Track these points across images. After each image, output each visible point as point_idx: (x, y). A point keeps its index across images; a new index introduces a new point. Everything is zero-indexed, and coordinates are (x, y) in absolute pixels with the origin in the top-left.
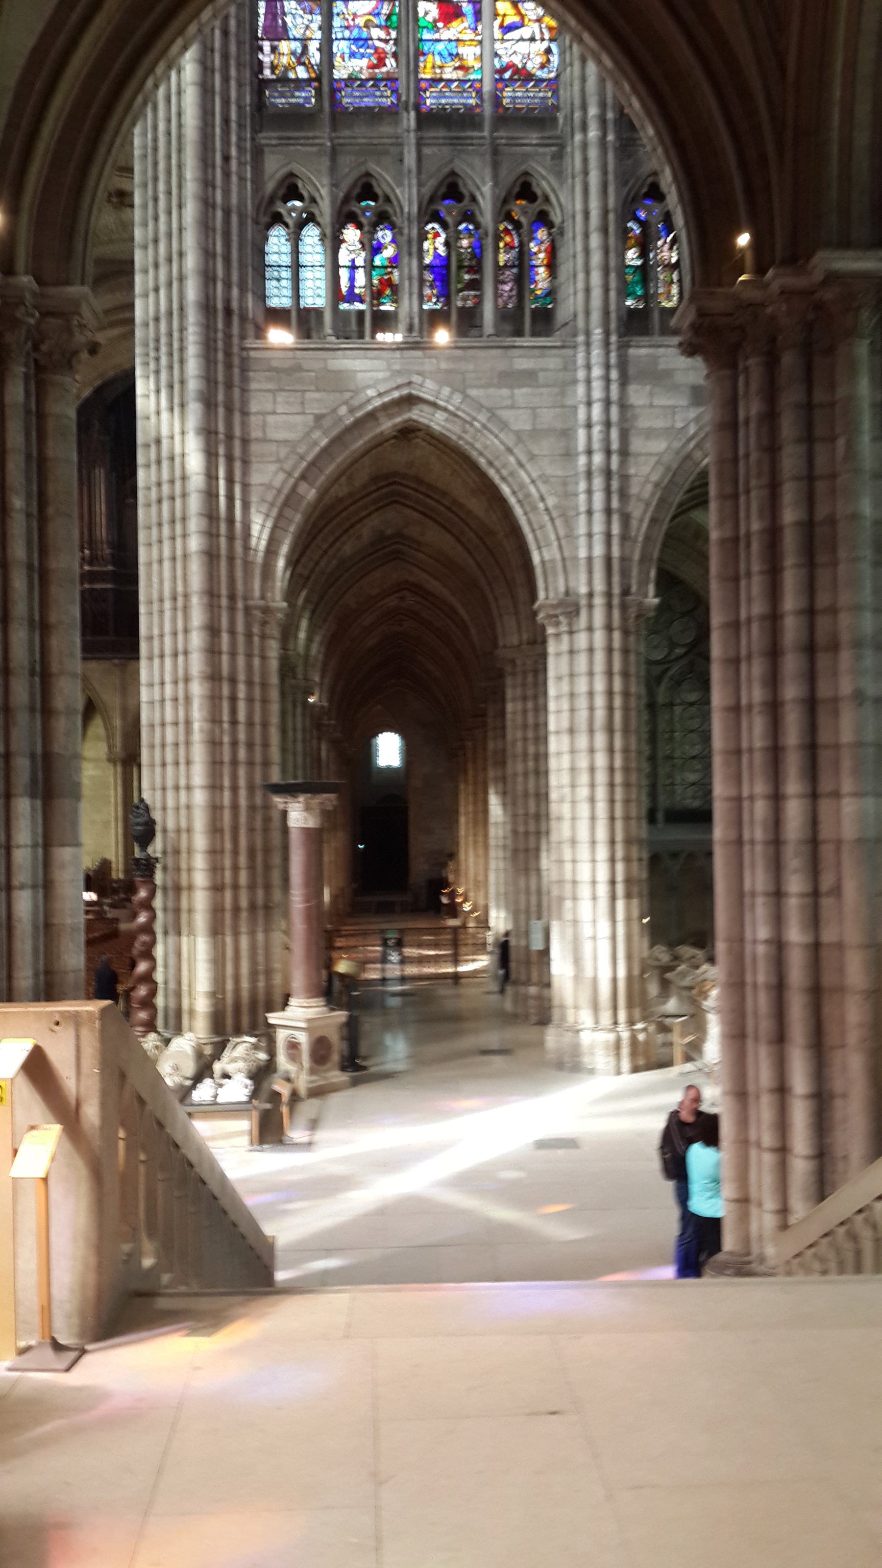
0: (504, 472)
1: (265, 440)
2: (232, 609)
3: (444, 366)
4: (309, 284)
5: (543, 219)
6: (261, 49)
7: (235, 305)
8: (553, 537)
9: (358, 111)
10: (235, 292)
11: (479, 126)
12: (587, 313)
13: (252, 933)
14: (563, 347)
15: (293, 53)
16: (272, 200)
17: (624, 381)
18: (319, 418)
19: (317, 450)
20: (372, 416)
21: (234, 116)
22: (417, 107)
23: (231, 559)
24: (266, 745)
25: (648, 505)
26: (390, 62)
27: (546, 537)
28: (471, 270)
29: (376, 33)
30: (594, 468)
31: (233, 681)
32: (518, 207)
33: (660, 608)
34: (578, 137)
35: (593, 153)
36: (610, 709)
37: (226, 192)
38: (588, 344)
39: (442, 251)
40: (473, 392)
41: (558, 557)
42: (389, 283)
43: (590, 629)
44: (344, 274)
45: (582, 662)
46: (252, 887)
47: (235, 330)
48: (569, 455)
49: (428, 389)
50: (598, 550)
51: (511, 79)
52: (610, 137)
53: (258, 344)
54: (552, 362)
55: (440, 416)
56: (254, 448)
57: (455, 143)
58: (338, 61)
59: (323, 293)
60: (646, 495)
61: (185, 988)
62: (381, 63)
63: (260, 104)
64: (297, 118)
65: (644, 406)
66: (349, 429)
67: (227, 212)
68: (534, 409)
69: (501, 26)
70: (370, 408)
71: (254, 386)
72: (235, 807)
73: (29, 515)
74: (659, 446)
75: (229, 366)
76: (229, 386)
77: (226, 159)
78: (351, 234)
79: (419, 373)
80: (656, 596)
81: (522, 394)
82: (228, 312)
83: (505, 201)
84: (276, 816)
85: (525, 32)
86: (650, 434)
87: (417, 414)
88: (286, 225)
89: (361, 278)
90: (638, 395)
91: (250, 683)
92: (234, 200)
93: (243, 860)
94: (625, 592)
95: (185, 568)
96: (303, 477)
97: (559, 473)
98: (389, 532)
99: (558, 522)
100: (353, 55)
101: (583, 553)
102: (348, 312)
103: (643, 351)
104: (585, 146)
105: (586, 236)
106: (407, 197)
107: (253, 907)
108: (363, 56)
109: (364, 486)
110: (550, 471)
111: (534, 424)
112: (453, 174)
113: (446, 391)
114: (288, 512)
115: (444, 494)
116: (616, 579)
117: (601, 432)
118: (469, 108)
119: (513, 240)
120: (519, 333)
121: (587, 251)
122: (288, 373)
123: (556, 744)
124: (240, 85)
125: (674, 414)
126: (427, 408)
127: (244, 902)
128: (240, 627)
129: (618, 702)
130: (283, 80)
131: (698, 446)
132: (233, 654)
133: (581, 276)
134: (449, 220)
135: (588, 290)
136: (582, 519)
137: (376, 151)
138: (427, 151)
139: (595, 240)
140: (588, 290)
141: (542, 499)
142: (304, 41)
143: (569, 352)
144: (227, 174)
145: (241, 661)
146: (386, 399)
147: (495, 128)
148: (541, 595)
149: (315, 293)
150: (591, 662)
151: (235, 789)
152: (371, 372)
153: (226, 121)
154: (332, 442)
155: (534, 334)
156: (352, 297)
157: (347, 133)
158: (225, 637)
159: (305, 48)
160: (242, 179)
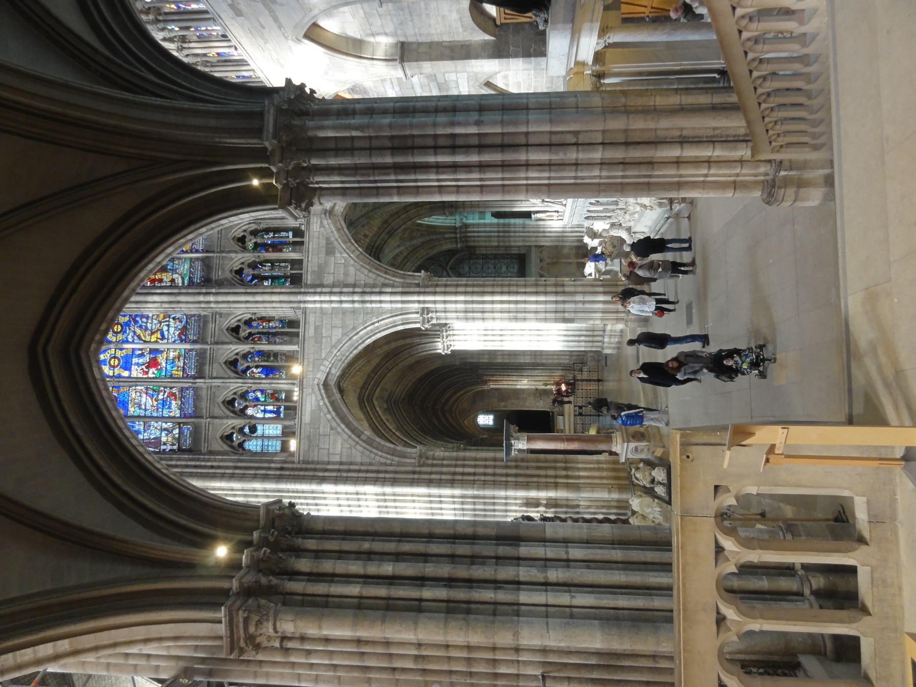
1: (341, 455)
2: (420, 473)
3: (311, 369)
4: (271, 432)
5: (248, 323)
6: (164, 450)
7: (278, 466)
8: (391, 319)
9: (195, 406)
10: (273, 465)
11: (205, 351)
12: (291, 302)
13: (579, 469)
15: (167, 435)
16: (232, 447)
17: (322, 285)
18: (332, 428)
20: (332, 403)
21: (193, 463)
22: (195, 378)
23: (396, 472)
24: (486, 460)
26: (174, 390)
28: (269, 356)
29: (161, 397)
31: (454, 474)
32: (244, 333)
33: (427, 270)
34: (213, 305)
37: (227, 468)
38: (305, 302)
39: (260, 370)
40: (323, 355)
42: (272, 395)
44: (268, 415)
46: (555, 468)
47: (290, 466)
48: (354, 311)
49: (322, 377)
52: (214, 291)
53: (297, 455)
54: (311, 318)
55: (333, 371)
56: (344, 460)
57: (212, 361)
58: (172, 414)
59: (275, 426)
60: (374, 276)
61: (606, 504)
62: (174, 395)
63: (189, 451)
64: (196, 433)
66: (338, 414)
67: (236, 468)
69: (162, 339)
71: (316, 459)
72: (516, 475)
73: (373, 540)
75: (306, 470)
76: (315, 470)
77: (212, 467)
78: (250, 411)
82: (282, 469)
83: (239, 339)
84: (520, 456)
85: (165, 328)
87: (332, 383)
88: (244, 441)
89: (270, 408)
90: (329, 279)
91: (456, 466)
92: (231, 464)
93: (542, 472)
94: (418, 285)
95: (399, 495)
98: (385, 406)
100: (170, 408)
102: (285, 414)
106: (235, 385)
107: (566, 469)
108: (170, 403)
109: (364, 414)
112: (225, 363)
114: (375, 444)
115: (369, 376)
116: (412, 290)
118: (197, 355)
120: (297, 335)
122: (310, 441)
124: (179, 460)
126: (330, 378)
127: (564, 473)
128: (429, 469)
129: (470, 289)
130: (179, 440)
132: (442, 473)
133: (274, 305)
134: (246, 365)
135: (281, 302)
137: (212, 398)
138: (215, 375)
140: (281, 302)
142: (162, 430)
143: (308, 311)
144: (219, 467)
145: (445, 469)
147: (206, 343)
148: (418, 326)
149: (274, 429)
151: (507, 475)
152: (312, 404)
153: (195, 467)
155: (298, 327)
156: (277, 412)
157: (204, 411)
158: (433, 476)
159: (165, 429)
160: (222, 460)
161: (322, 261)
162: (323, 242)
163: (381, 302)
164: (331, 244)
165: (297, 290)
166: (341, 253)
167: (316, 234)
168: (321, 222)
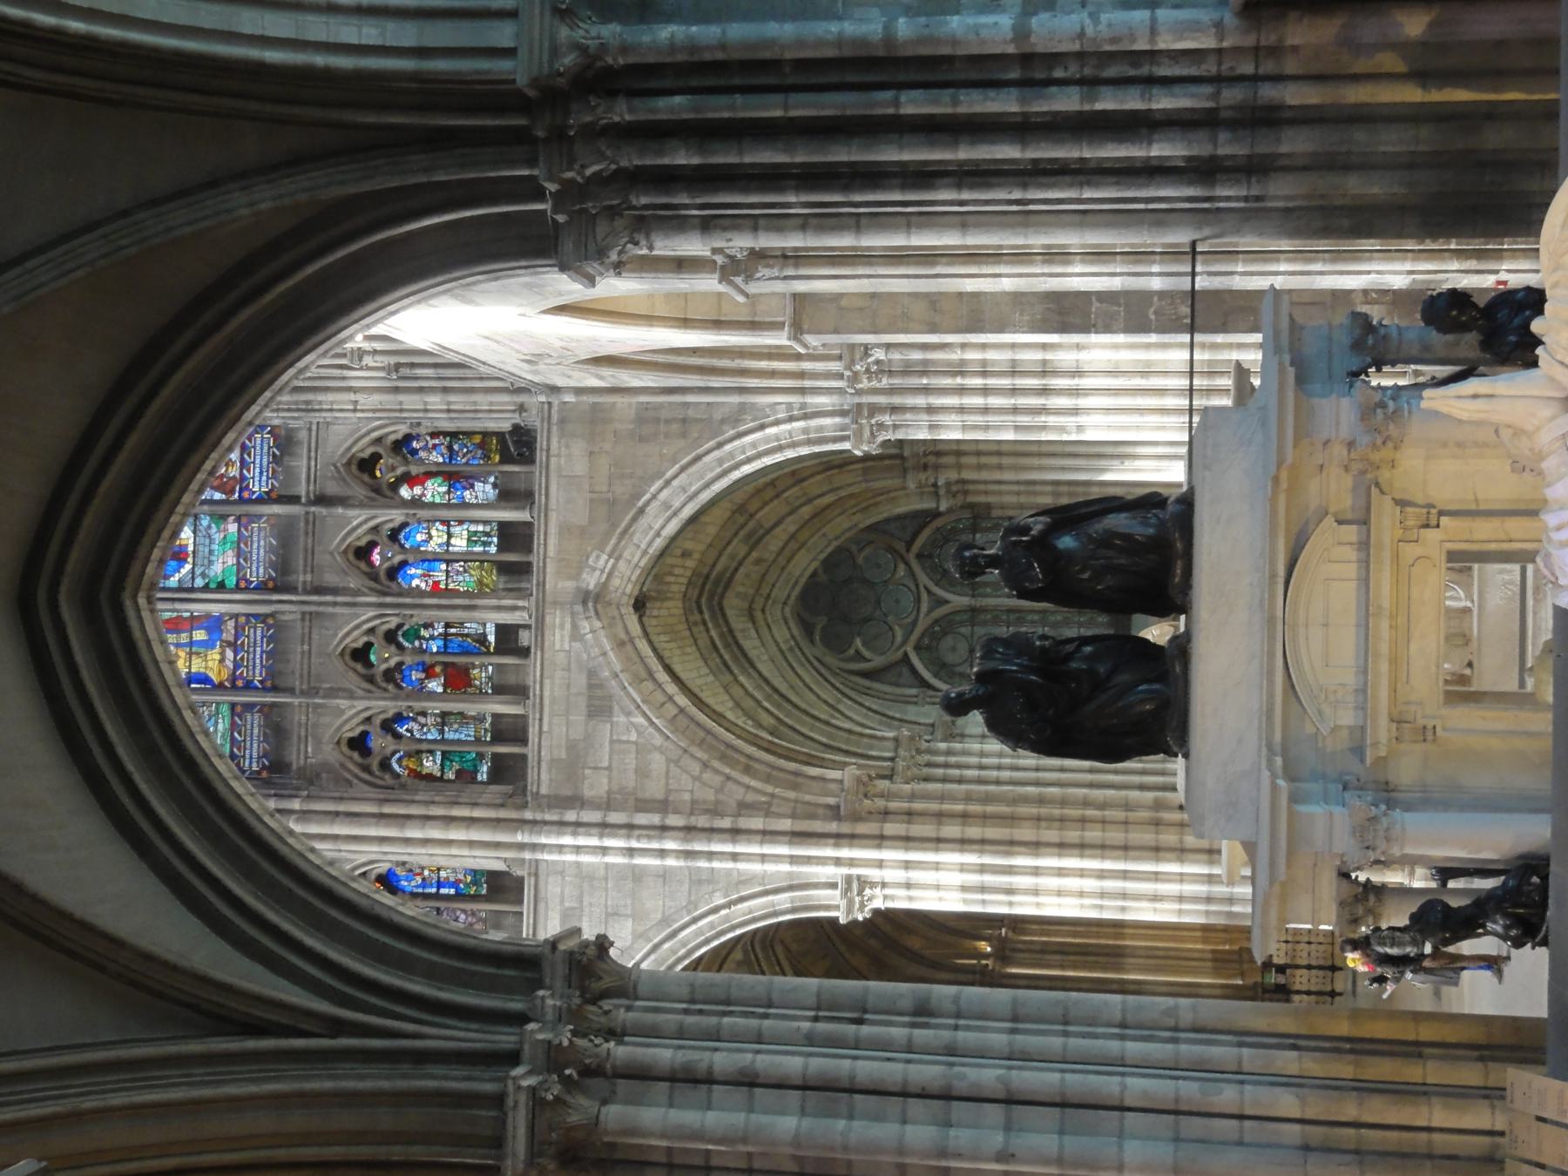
12: (497, 845)
14: (536, 875)
38: (534, 847)
48: (664, 875)
52: (296, 805)
65: (610, 778)
68: (608, 915)
90: (596, 785)
94: (835, 813)
103: (544, 776)
105: (407, 841)
121: (426, 842)
123: (1025, 907)
129: (974, 832)
140: (471, 844)
143: (542, 867)
161: (577, 733)
162: (581, 681)
163: (735, 857)
164: (601, 686)
165: (513, 815)
166: (628, 714)
167: (561, 658)
168: (575, 627)
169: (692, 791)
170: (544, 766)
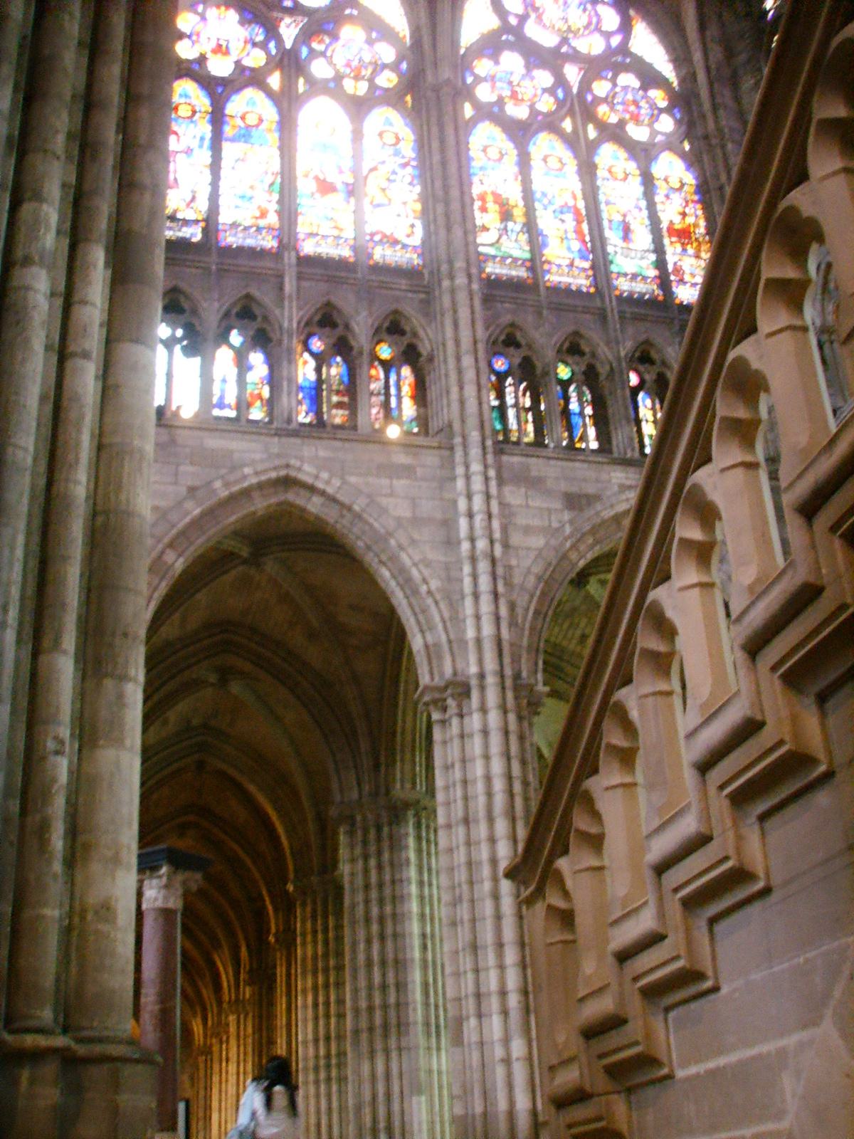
0: (384, 558)
8: (437, 619)
17: (501, 482)
18: (192, 490)
19: (187, 519)
20: (246, 493)
25: (532, 596)
27: (429, 621)
30: (478, 552)
35: (462, 297)
36: (511, 795)
38: (465, 445)
41: (444, 638)
43: (483, 710)
45: (476, 745)
48: (451, 543)
50: (488, 629)
51: (381, 240)
55: (317, 500)
62: (263, 214)
65: (520, 506)
68: (413, 500)
70: (246, 484)
74: (538, 542)
79: (296, 457)
80: (545, 684)
81: (400, 484)
86: (527, 530)
94: (517, 676)
96: (171, 545)
97: (442, 558)
99: (442, 605)
101: (470, 633)
103: (516, 459)
104: (453, 291)
110: (432, 555)
111: (414, 512)
113: (325, 475)
117: (482, 520)
119: (378, 373)
125: (550, 514)
129: (517, 787)
131: (573, 547)
136: (469, 602)
139: (467, 361)
141: (425, 581)
146: (263, 478)
150: (486, 746)
154: (203, 515)
161: (550, 484)
162: (590, 489)
164: (589, 504)
167: (604, 476)
168: (630, 487)
169: (518, 566)
170: (523, 459)
